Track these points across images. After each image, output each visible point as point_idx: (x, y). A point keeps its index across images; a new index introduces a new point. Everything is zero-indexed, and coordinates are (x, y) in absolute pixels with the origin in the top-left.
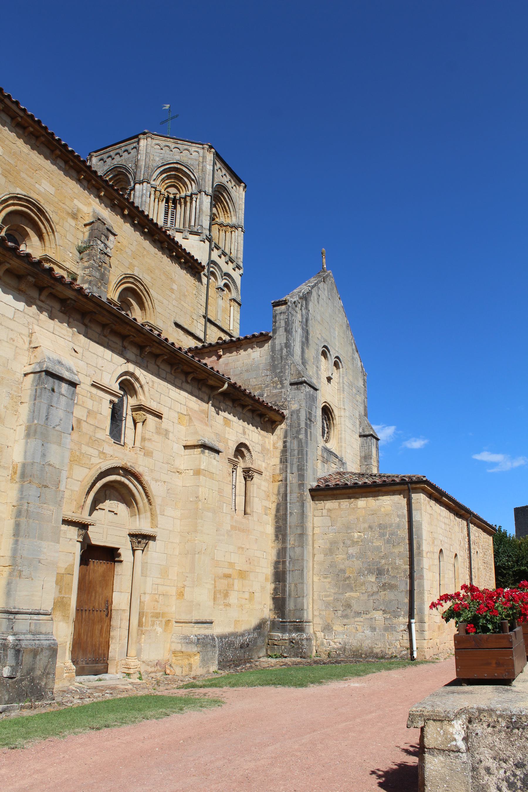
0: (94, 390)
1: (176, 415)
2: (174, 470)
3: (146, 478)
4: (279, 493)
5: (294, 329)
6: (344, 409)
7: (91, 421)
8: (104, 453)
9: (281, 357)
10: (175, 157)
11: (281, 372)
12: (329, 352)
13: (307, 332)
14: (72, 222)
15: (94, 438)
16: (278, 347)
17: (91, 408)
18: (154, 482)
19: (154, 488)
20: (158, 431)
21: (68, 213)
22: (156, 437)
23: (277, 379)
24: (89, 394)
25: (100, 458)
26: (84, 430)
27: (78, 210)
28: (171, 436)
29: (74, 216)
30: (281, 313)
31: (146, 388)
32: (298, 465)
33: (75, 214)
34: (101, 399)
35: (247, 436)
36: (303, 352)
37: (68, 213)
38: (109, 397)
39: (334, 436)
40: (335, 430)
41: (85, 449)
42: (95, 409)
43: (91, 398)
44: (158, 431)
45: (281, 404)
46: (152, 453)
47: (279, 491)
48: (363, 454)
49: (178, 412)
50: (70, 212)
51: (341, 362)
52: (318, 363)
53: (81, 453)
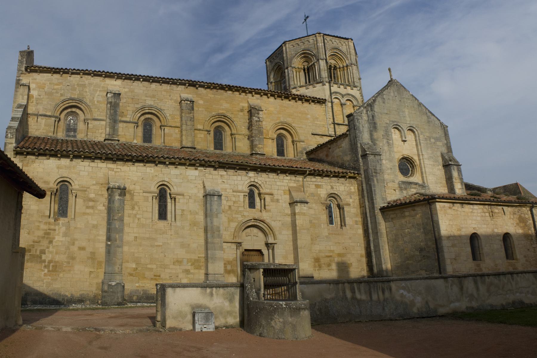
0: (235, 194)
1: (282, 191)
2: (285, 215)
3: (267, 221)
4: (363, 213)
5: (361, 126)
6: (422, 155)
7: (235, 205)
8: (244, 216)
9: (355, 144)
10: (302, 47)
11: (356, 151)
12: (400, 126)
13: (375, 123)
14: (241, 114)
15: (238, 211)
16: (352, 139)
17: (234, 200)
18: (273, 222)
19: (273, 224)
20: (272, 200)
21: (238, 111)
22: (271, 203)
23: (354, 155)
24: (233, 196)
25: (242, 218)
26: (233, 209)
27: (243, 107)
28: (280, 201)
29: (242, 110)
30: (351, 121)
31: (262, 185)
32: (371, 198)
33: (242, 109)
34: (239, 196)
35: (335, 189)
36: (371, 135)
37: (238, 111)
38: (243, 194)
39: (416, 172)
40: (417, 168)
41: (234, 216)
42: (237, 200)
43: (234, 196)
44: (272, 200)
45: (358, 167)
46: (270, 210)
47: (363, 212)
48: (447, 177)
49: (283, 190)
50: (239, 110)
51: (415, 128)
52: (388, 136)
53: (233, 218)
